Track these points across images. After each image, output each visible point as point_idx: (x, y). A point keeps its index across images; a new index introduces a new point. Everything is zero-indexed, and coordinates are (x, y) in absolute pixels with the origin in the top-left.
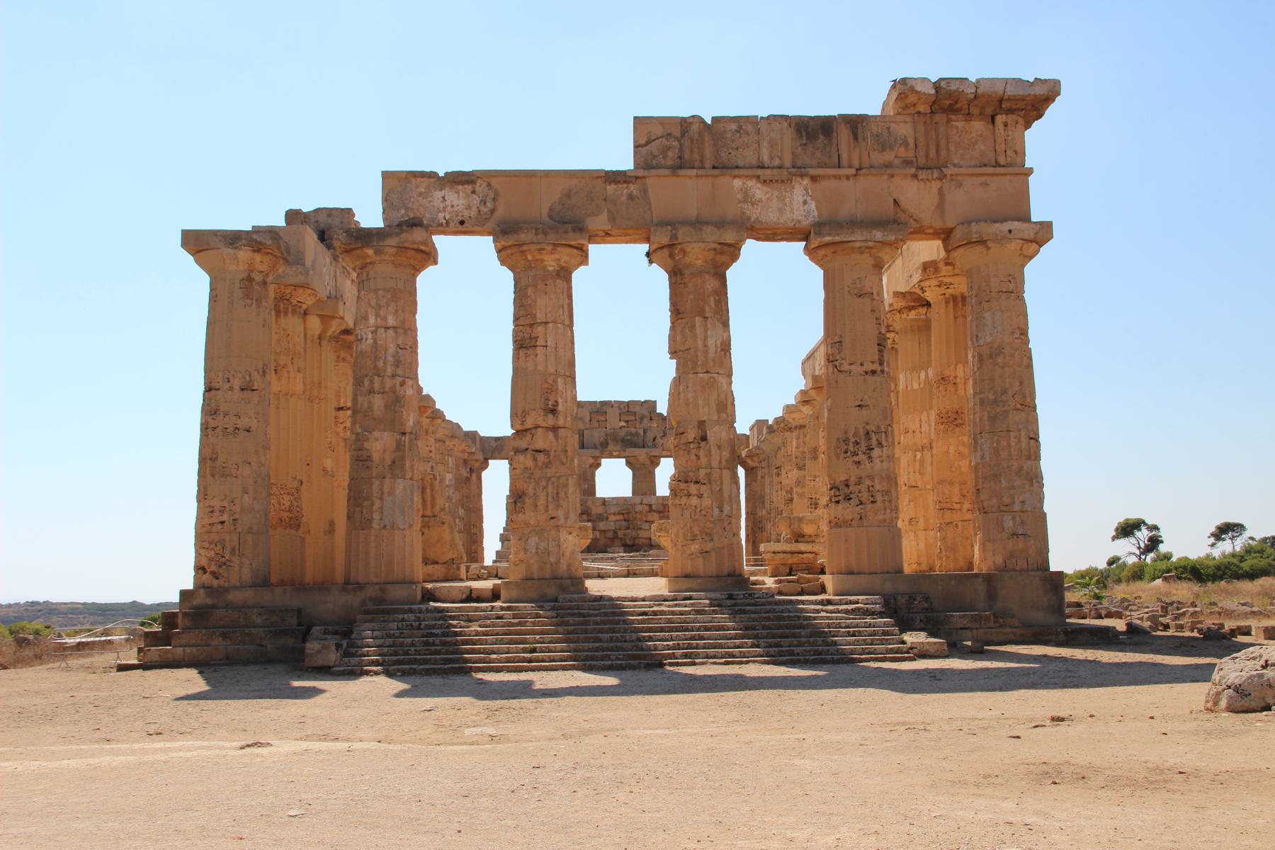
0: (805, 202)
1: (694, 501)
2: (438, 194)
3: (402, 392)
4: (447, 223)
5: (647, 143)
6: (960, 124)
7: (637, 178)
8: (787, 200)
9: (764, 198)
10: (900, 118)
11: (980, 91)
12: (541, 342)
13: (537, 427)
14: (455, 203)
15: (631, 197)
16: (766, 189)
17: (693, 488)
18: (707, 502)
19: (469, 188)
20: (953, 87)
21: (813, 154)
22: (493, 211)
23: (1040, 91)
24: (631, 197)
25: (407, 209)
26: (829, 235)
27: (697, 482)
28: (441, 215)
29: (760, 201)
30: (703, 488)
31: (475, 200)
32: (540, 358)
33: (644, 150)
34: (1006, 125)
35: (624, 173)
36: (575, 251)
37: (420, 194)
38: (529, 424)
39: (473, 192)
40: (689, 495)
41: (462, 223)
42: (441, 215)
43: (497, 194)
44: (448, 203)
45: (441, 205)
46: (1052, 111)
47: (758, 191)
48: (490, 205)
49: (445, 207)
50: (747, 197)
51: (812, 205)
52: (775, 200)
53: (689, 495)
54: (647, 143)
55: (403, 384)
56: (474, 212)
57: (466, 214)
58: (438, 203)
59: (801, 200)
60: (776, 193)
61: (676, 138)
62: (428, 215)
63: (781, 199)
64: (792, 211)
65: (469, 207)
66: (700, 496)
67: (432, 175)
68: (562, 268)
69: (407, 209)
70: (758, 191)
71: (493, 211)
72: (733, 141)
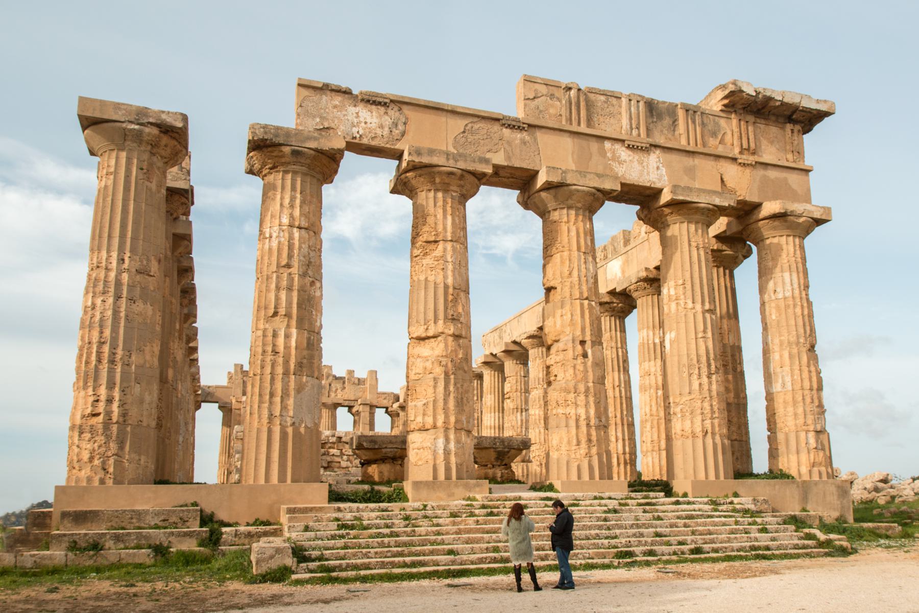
0: (658, 168)
2: (352, 110)
3: (312, 292)
4: (361, 136)
6: (762, 126)
7: (530, 126)
8: (645, 164)
9: (628, 159)
10: (722, 114)
11: (785, 100)
14: (369, 121)
16: (630, 152)
19: (382, 109)
20: (768, 94)
21: (662, 131)
23: (823, 107)
24: (524, 142)
26: (682, 195)
28: (355, 130)
29: (625, 161)
31: (387, 121)
33: (533, 104)
34: (792, 131)
35: (516, 120)
37: (335, 107)
39: (386, 113)
41: (373, 138)
42: (355, 130)
43: (407, 119)
44: (362, 119)
45: (355, 120)
46: (818, 128)
47: (623, 153)
48: (401, 127)
49: (360, 122)
50: (616, 158)
51: (663, 171)
52: (636, 163)
55: (312, 284)
56: (386, 131)
57: (379, 132)
58: (351, 117)
59: (655, 166)
60: (637, 157)
62: (342, 128)
63: (641, 163)
64: (648, 174)
65: (381, 127)
67: (347, 92)
70: (623, 153)
72: (602, 109)
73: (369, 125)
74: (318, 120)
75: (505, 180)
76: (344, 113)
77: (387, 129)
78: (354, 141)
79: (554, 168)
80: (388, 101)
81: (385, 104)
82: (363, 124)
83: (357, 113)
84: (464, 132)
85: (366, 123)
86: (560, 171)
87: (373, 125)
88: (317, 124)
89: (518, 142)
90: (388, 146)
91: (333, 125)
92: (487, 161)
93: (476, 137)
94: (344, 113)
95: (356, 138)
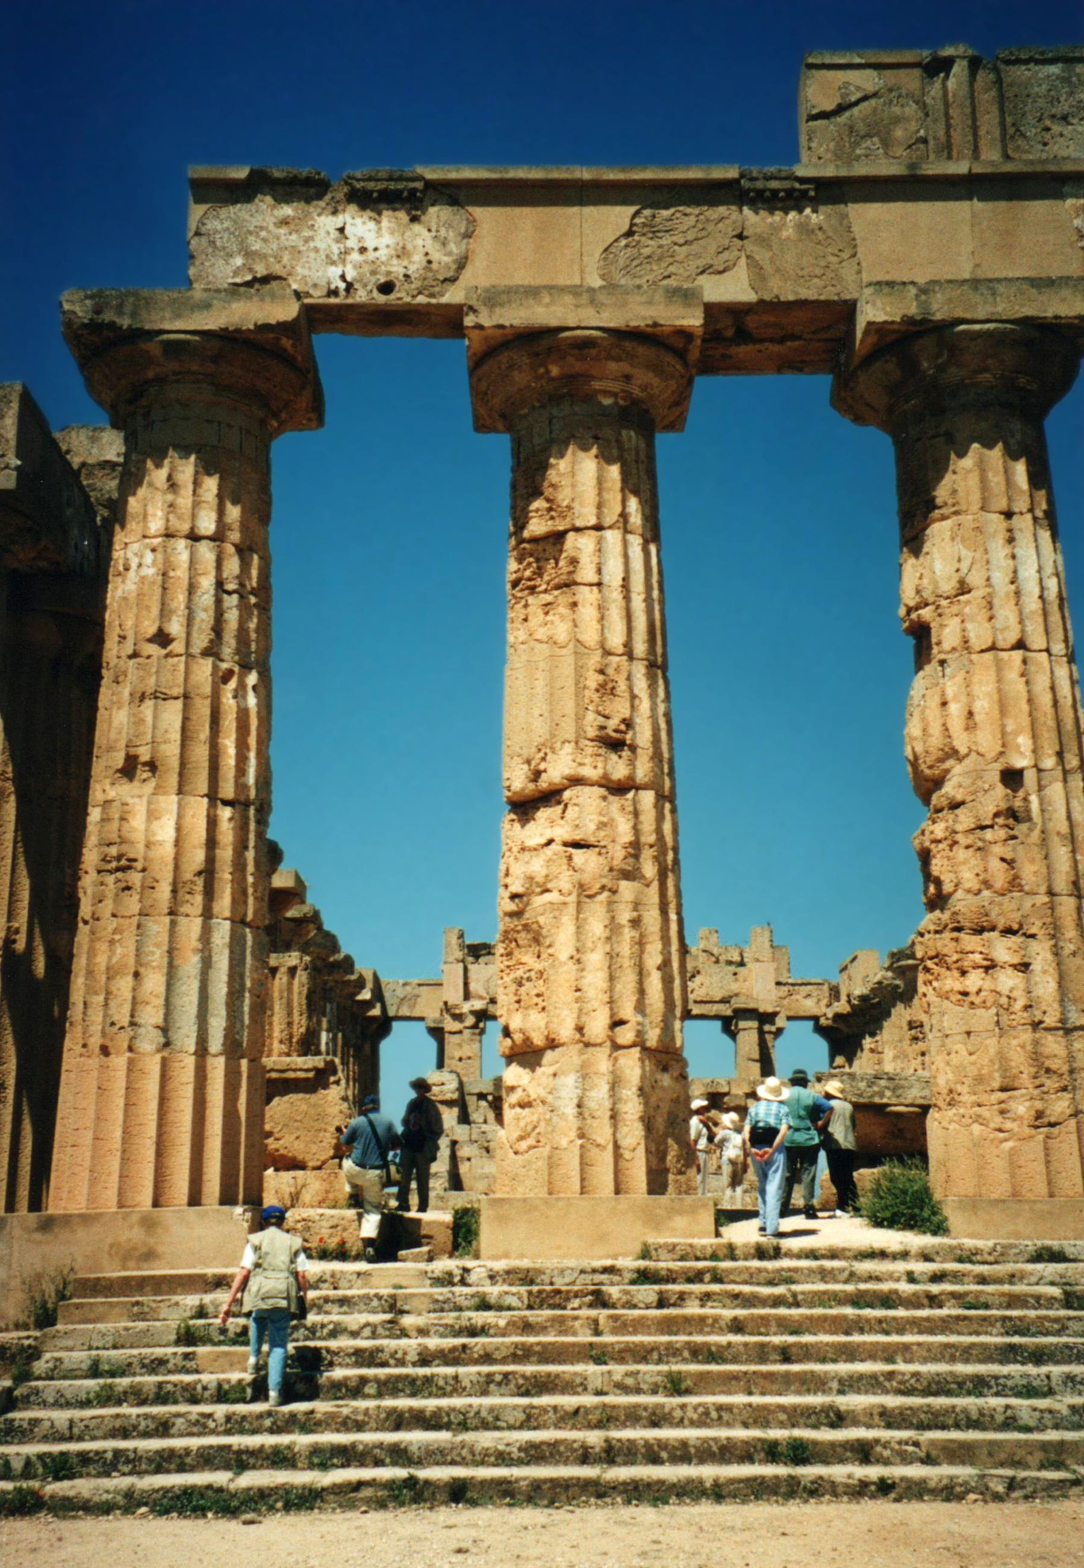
1: (1008, 981)
2: (326, 223)
4: (349, 286)
5: (841, 109)
12: (586, 573)
13: (576, 781)
14: (370, 244)
15: (804, 229)
17: (1003, 950)
18: (1046, 987)
22: (462, 264)
25: (248, 254)
27: (1008, 931)
28: (334, 272)
30: (1034, 946)
32: (588, 613)
36: (669, 358)
37: (285, 222)
38: (556, 771)
40: (990, 967)
41: (386, 288)
44: (352, 243)
45: (335, 249)
49: (347, 252)
53: (990, 967)
54: (841, 109)
57: (397, 269)
61: (910, 95)
65: (402, 253)
66: (1024, 967)
68: (635, 402)
69: (248, 254)
71: (462, 264)
72: (1055, 101)
73: (371, 255)
74: (239, 261)
75: (775, 348)
76: (307, 233)
77: (418, 259)
78: (333, 300)
79: (890, 284)
80: (419, 185)
81: (413, 191)
82: (355, 256)
83: (341, 230)
84: (630, 233)
85: (363, 250)
86: (913, 291)
87: (383, 254)
88: (236, 273)
89: (788, 232)
90: (421, 299)
91: (277, 269)
92: (685, 296)
93: (666, 241)
94: (307, 233)
95: (334, 293)
